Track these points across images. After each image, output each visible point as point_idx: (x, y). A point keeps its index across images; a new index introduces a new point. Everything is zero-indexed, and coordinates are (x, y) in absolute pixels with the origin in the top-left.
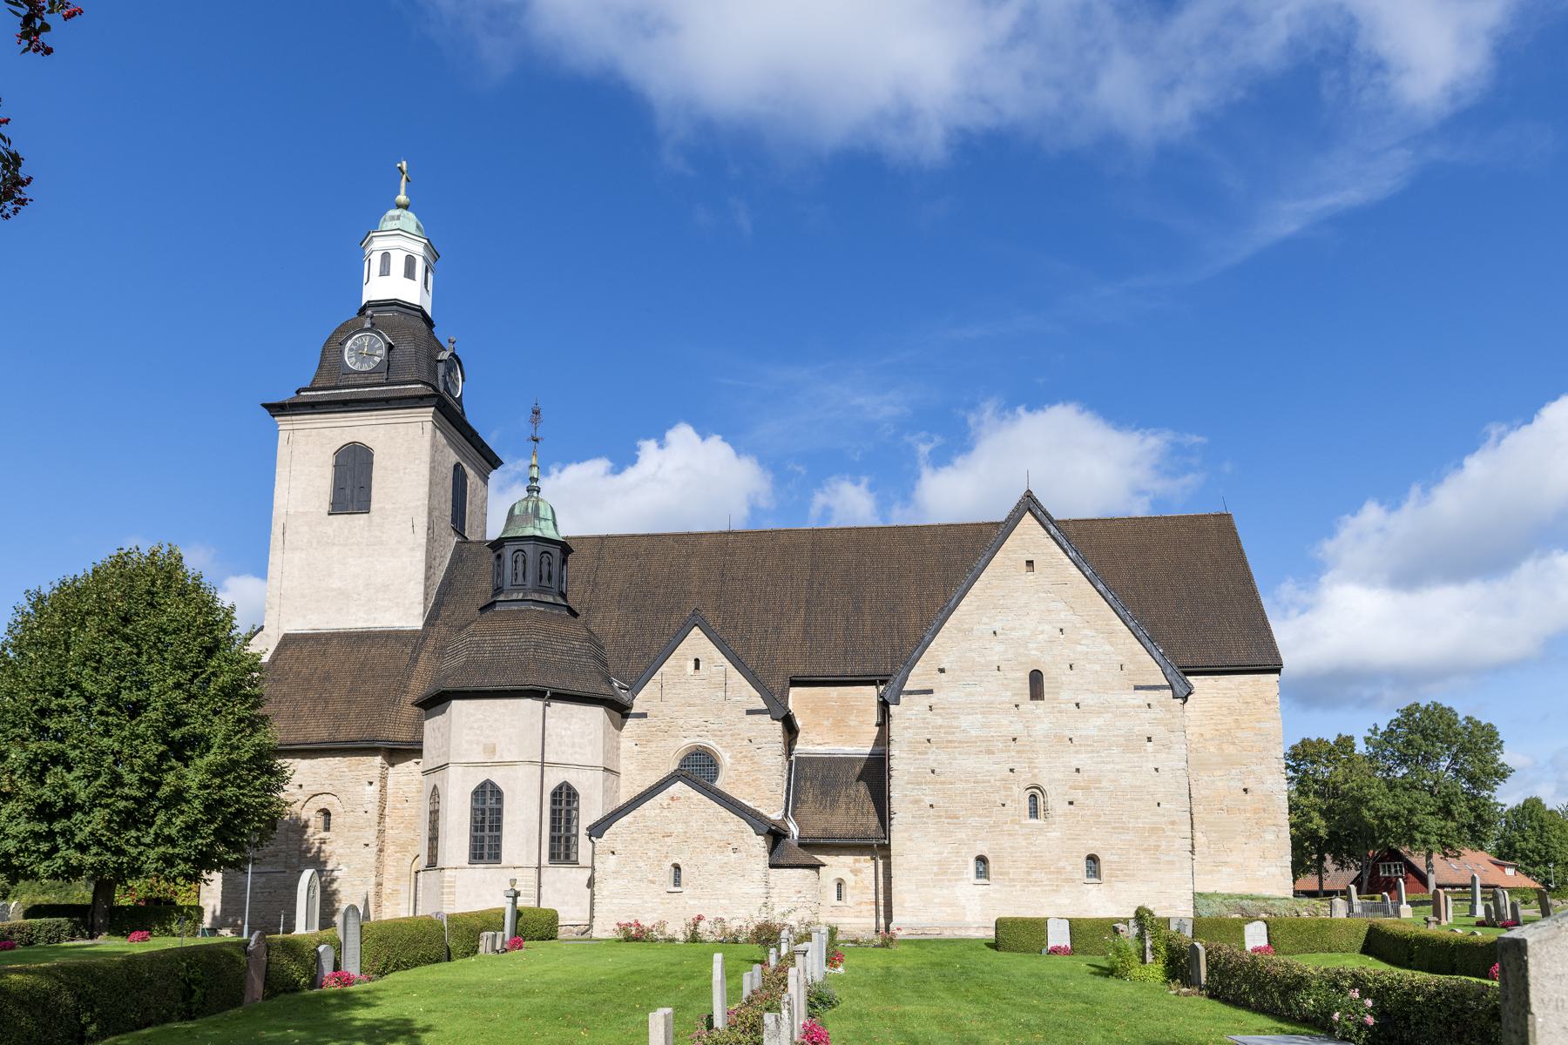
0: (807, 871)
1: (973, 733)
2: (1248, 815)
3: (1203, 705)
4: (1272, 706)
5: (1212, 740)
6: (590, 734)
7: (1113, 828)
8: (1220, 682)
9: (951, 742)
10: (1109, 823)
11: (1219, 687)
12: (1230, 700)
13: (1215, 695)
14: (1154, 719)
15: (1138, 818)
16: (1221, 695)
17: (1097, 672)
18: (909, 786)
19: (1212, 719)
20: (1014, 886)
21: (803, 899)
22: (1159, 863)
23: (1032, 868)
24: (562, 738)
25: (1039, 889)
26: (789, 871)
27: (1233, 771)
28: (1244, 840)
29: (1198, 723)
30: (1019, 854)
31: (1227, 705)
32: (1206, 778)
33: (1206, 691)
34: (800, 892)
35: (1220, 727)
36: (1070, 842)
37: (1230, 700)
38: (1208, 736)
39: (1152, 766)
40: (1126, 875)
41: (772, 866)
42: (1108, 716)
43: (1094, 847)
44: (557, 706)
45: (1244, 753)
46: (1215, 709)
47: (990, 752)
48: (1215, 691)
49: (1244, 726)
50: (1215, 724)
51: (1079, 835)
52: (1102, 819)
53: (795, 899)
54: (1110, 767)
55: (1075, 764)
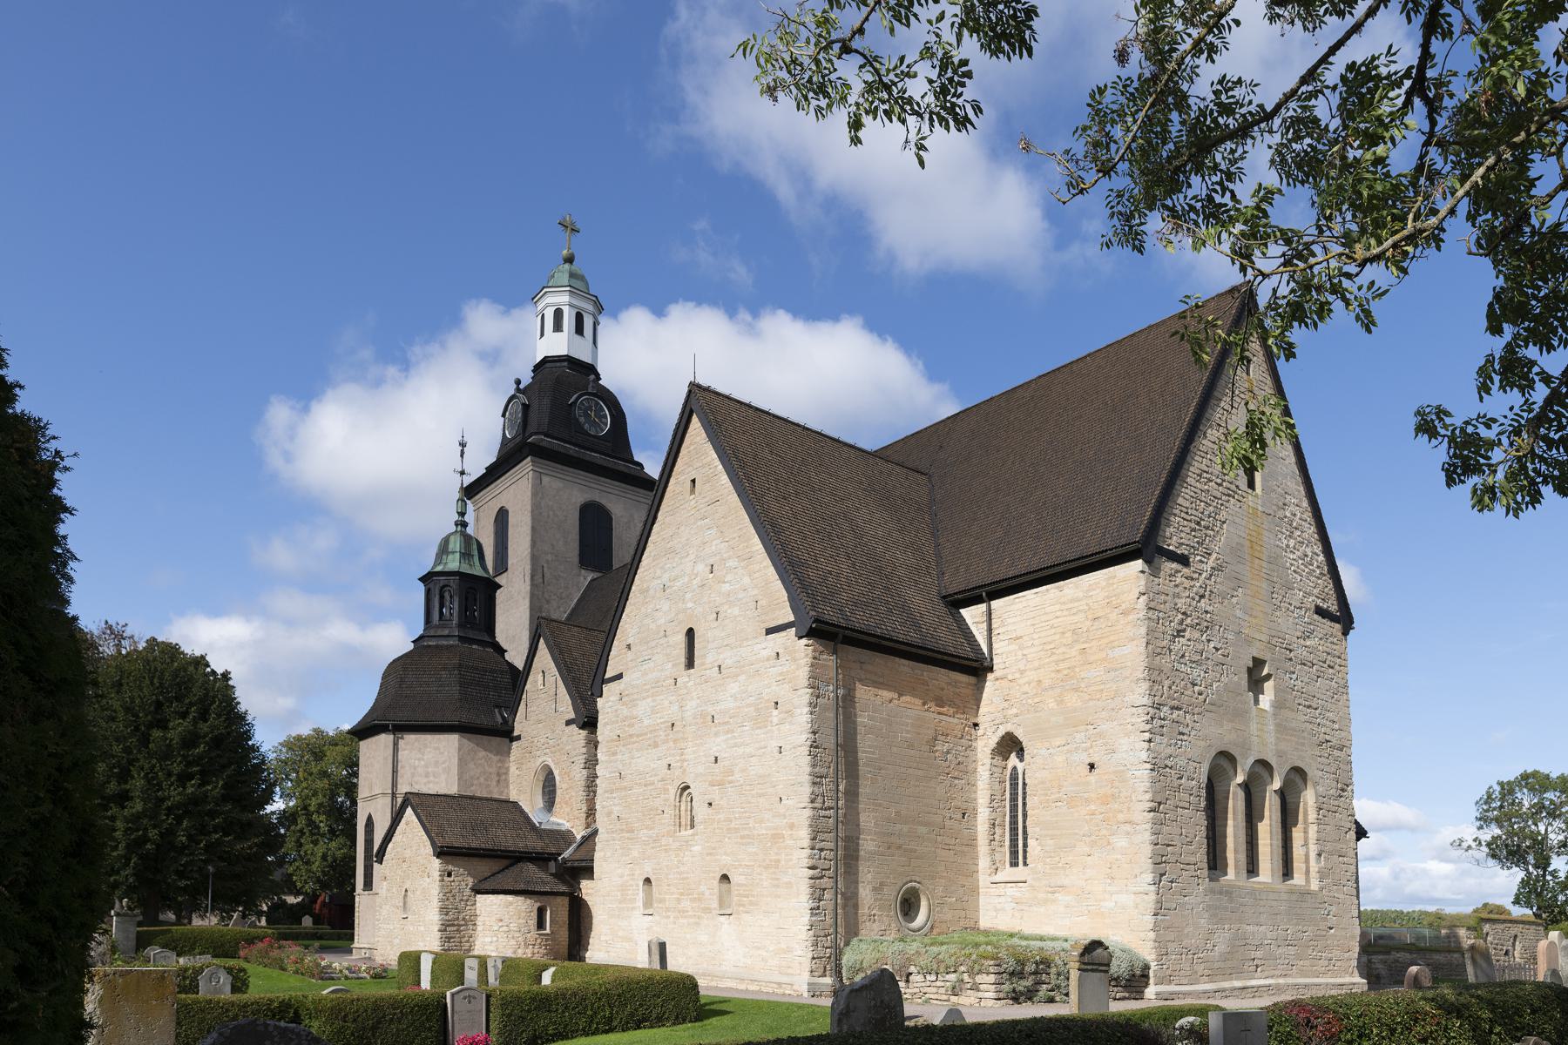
0: (510, 898)
1: (646, 722)
2: (1093, 807)
3: (1043, 634)
4: (1131, 617)
5: (1052, 688)
6: (443, 763)
7: (742, 837)
8: (1066, 591)
9: (631, 736)
10: (736, 830)
11: (1062, 600)
12: (1075, 618)
13: (1058, 614)
14: (781, 674)
15: (761, 822)
16: (1065, 613)
17: (735, 617)
18: (606, 795)
19: (1053, 654)
20: (668, 917)
21: (505, 928)
22: (778, 886)
23: (682, 894)
24: (415, 768)
25: (685, 921)
26: (491, 897)
27: (1078, 736)
28: (1087, 849)
29: (1036, 664)
30: (671, 876)
31: (1073, 627)
32: (1043, 752)
33: (1048, 610)
34: (501, 920)
35: (1062, 666)
36: (708, 858)
37: (1075, 618)
38: (1047, 683)
39: (775, 744)
40: (751, 903)
41: (478, 891)
42: (743, 678)
43: (725, 862)
44: (410, 739)
45: (1091, 703)
46: (1057, 636)
47: (656, 745)
48: (1057, 607)
49: (1092, 659)
50: (1057, 662)
51: (714, 849)
52: (733, 825)
53: (496, 928)
54: (741, 750)
55: (714, 751)
